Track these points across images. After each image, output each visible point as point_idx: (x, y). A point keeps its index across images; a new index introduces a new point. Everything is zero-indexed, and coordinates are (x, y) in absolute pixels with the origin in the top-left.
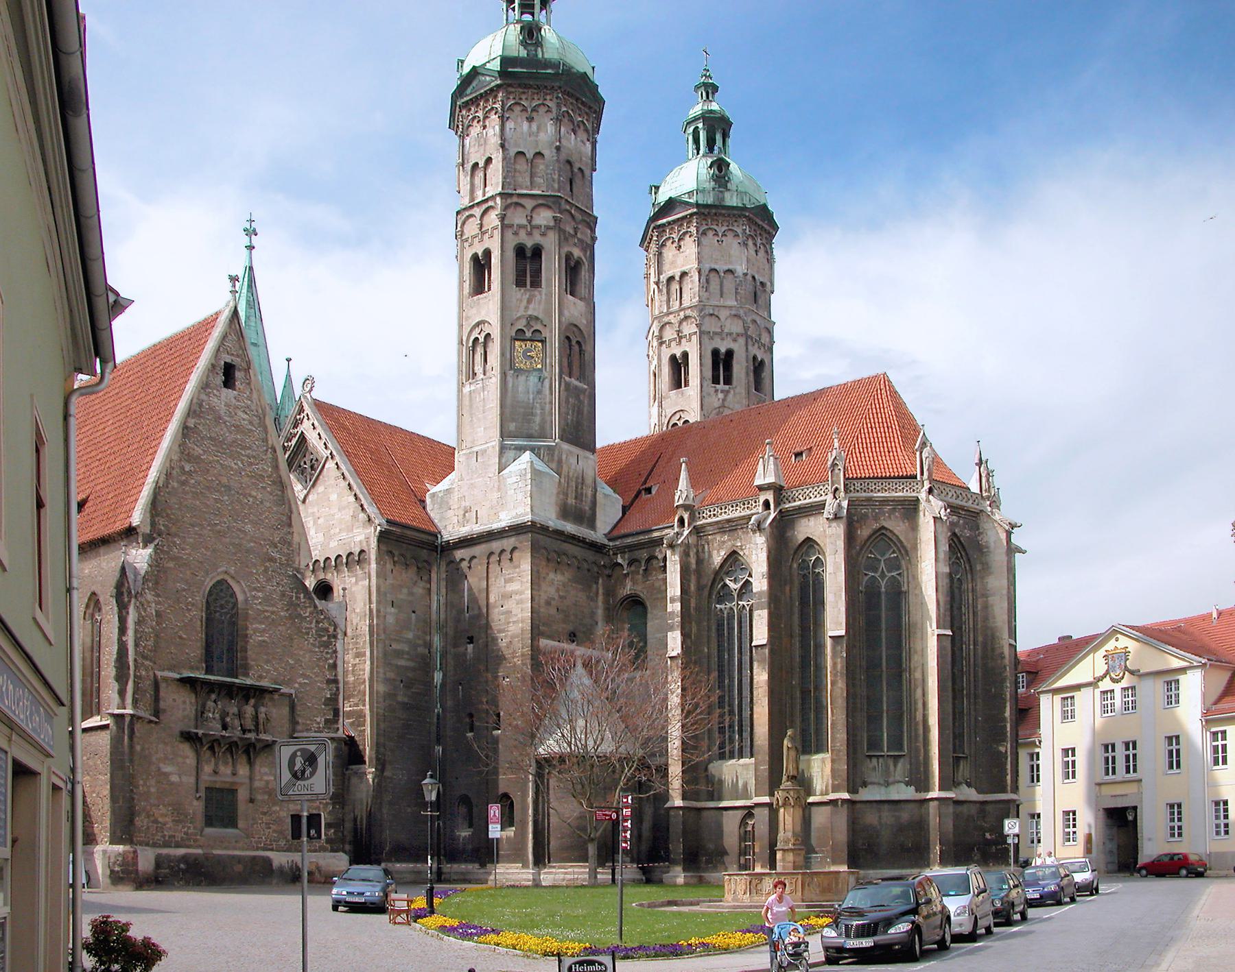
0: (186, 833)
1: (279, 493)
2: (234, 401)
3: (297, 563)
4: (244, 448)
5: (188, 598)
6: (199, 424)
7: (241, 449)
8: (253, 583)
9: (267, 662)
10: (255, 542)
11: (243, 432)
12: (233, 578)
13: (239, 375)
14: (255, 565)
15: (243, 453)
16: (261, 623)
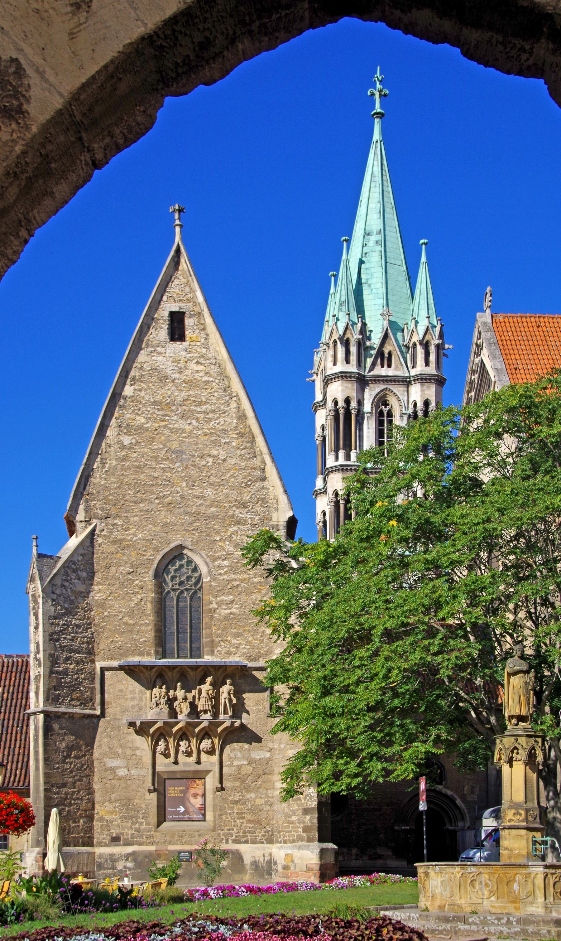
0: (138, 830)
1: (249, 445)
2: (184, 353)
3: (274, 519)
4: (200, 404)
5: (134, 581)
6: (140, 390)
7: (196, 406)
8: (215, 552)
9: (238, 635)
10: (216, 506)
11: (197, 386)
12: (191, 550)
13: (189, 322)
14: (218, 532)
15: (199, 409)
16: (228, 594)
